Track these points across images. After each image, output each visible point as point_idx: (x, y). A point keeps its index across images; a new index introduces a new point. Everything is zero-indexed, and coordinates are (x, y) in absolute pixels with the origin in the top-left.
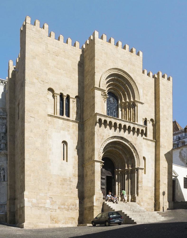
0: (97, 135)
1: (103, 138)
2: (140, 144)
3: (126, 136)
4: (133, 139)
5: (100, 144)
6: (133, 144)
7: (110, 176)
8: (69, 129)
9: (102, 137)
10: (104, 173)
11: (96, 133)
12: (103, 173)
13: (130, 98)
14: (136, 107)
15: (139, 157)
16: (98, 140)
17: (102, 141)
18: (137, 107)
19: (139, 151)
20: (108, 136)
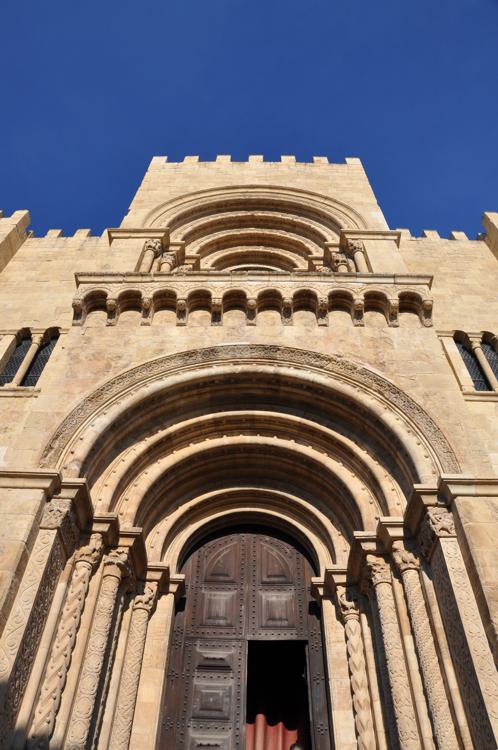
0: (75, 359)
1: (108, 366)
2: (419, 358)
3: (298, 338)
4: (359, 344)
5: (82, 392)
6: (359, 368)
7: (283, 637)
8: (10, 425)
9: (101, 364)
10: (229, 626)
11: (69, 354)
12: (219, 626)
13: (319, 239)
14: (359, 256)
15: (431, 421)
16: (72, 375)
17: (96, 380)
18: (364, 253)
19: (420, 389)
20: (150, 352)
